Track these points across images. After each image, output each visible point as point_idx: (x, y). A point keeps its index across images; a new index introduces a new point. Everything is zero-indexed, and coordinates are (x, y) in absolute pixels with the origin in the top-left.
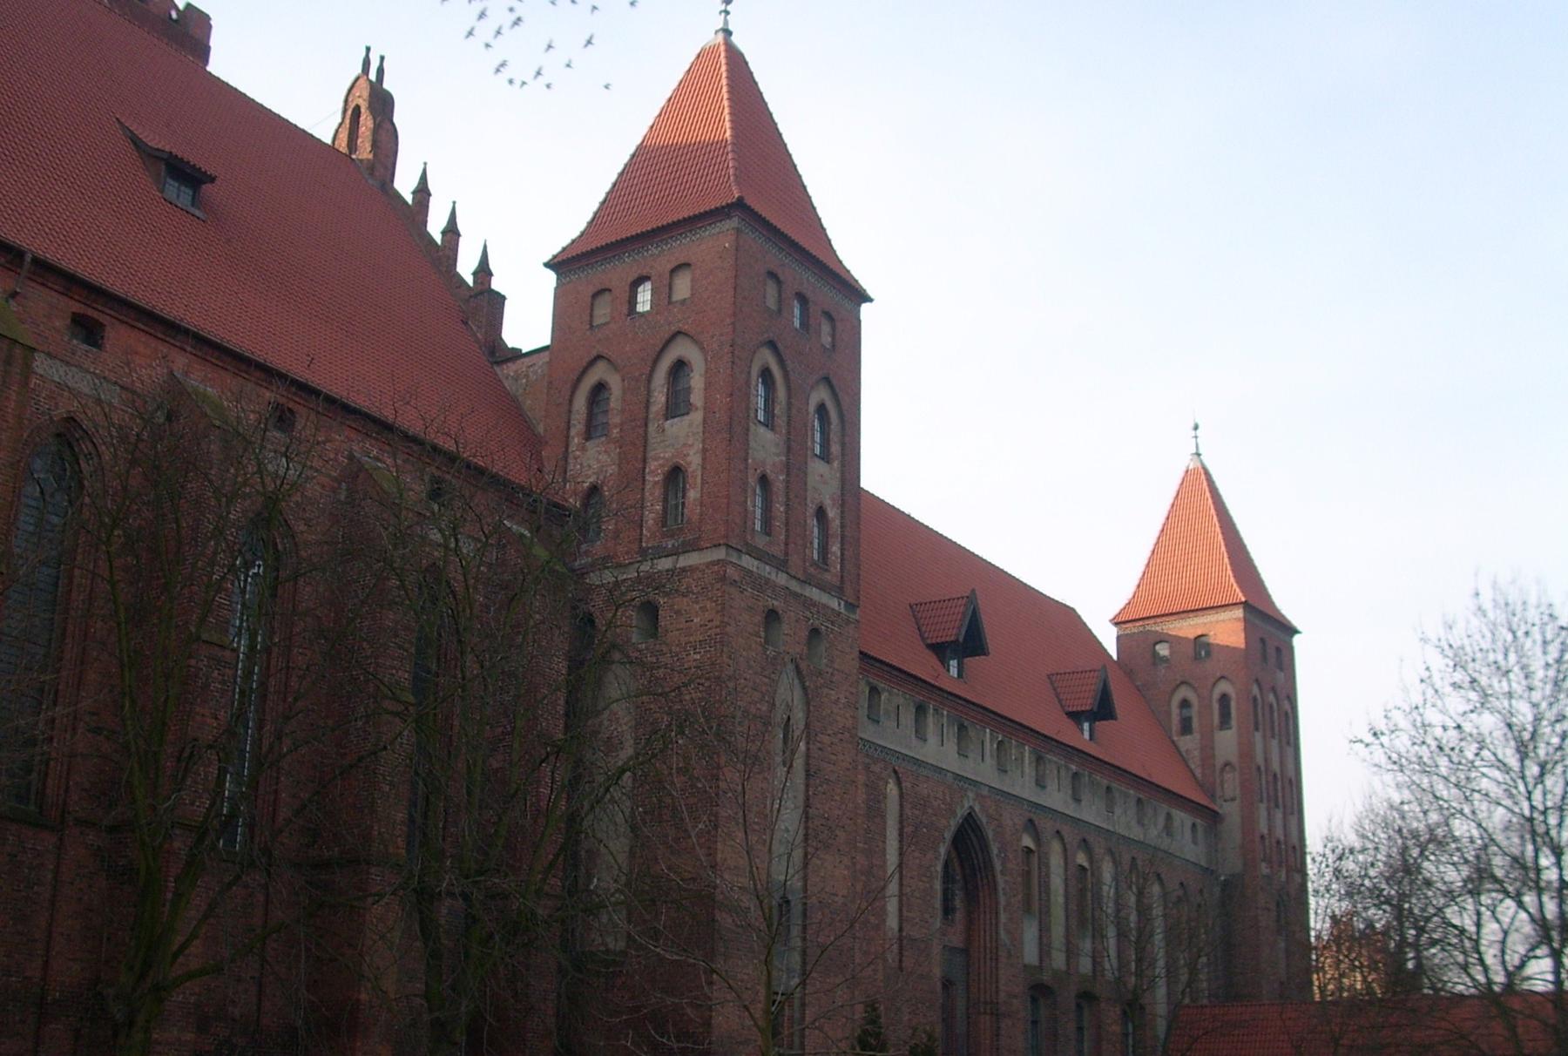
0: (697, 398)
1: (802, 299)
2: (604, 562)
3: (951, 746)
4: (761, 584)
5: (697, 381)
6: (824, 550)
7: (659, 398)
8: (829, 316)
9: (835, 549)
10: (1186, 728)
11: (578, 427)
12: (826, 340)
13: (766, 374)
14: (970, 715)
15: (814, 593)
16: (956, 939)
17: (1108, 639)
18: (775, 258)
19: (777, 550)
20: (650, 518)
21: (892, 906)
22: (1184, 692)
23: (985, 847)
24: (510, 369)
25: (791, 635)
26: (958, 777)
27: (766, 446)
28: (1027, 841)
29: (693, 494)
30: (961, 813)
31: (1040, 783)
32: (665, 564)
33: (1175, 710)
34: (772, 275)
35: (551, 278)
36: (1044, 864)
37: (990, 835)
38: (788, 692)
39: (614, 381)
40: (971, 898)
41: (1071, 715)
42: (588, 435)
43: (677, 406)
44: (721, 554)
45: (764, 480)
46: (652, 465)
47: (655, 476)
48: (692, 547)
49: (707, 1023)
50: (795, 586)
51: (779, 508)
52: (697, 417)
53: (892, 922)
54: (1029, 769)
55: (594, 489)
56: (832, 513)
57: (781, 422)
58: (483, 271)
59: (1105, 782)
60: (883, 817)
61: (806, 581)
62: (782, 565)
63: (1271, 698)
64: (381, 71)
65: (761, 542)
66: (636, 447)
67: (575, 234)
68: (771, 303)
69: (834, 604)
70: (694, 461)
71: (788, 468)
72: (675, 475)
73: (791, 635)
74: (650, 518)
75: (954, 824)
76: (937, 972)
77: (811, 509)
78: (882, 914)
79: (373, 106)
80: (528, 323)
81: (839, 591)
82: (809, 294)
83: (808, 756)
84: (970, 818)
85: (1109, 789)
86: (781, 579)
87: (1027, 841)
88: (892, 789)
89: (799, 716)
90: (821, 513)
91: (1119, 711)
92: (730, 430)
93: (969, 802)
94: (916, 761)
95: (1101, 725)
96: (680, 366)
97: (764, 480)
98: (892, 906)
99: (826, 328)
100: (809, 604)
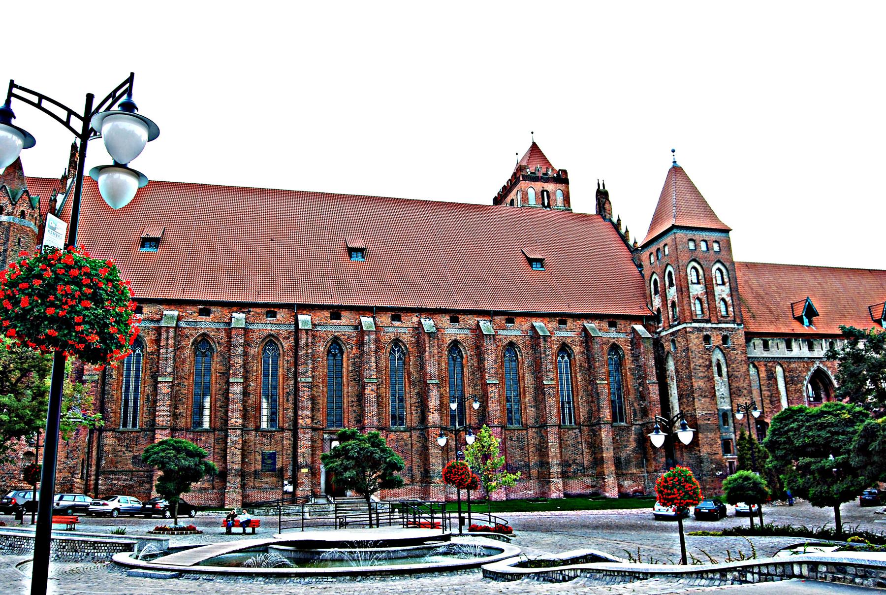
1: (706, 241)
3: (805, 349)
4: (700, 330)
6: (727, 311)
9: (731, 309)
11: (653, 292)
18: (690, 234)
19: (706, 318)
20: (670, 317)
25: (716, 340)
26: (809, 358)
34: (691, 240)
38: (718, 356)
42: (655, 294)
43: (671, 285)
44: (684, 325)
45: (698, 299)
48: (679, 324)
49: (699, 451)
50: (714, 326)
51: (705, 305)
52: (675, 287)
55: (659, 309)
56: (728, 299)
57: (702, 281)
60: (776, 379)
62: (708, 321)
65: (699, 317)
69: (732, 326)
71: (706, 293)
72: (673, 303)
73: (716, 340)
74: (670, 317)
81: (734, 322)
83: (728, 372)
86: (709, 325)
89: (722, 361)
90: (723, 300)
96: (670, 273)
97: (698, 299)
100: (720, 329)
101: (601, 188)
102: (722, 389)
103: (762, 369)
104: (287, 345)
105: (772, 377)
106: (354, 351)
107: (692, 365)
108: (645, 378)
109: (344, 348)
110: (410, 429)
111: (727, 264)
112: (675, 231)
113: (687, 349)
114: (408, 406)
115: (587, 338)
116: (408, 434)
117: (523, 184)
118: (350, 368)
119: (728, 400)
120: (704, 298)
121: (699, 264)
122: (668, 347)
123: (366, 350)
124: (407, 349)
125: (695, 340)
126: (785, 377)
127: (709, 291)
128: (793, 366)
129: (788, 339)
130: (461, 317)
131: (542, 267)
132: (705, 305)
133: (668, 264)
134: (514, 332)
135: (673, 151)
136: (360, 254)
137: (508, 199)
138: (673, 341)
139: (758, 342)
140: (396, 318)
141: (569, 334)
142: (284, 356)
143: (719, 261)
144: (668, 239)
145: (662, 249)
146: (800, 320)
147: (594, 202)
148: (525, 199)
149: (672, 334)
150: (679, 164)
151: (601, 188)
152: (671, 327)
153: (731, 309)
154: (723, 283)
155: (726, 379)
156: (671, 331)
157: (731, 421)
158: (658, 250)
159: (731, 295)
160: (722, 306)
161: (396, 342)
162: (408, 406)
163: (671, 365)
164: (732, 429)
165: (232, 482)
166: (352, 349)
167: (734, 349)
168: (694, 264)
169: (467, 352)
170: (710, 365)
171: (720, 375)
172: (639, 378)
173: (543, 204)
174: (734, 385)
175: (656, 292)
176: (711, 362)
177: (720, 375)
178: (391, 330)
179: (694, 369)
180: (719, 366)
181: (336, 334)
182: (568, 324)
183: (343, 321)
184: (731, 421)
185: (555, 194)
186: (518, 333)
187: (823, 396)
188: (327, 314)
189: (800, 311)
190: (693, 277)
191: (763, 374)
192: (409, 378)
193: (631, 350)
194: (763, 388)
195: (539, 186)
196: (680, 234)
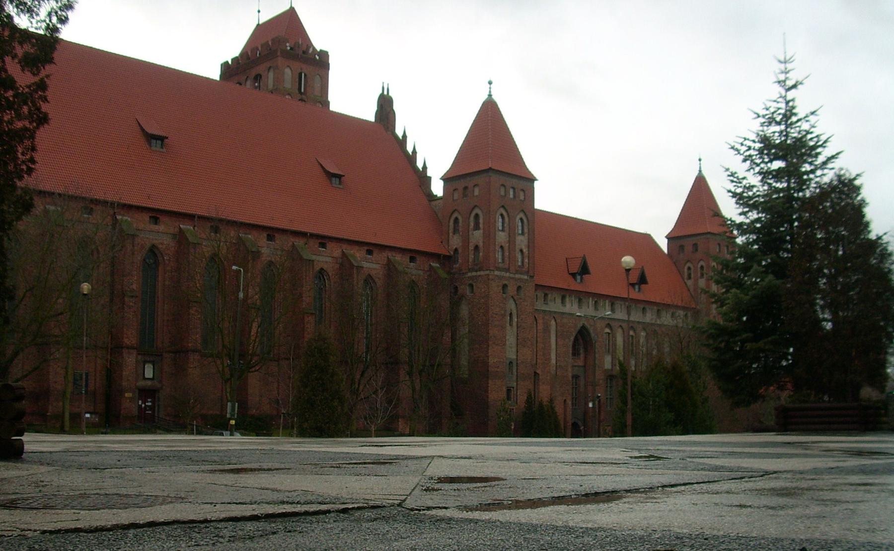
0: (481, 226)
1: (514, 188)
5: (481, 221)
6: (523, 262)
7: (472, 224)
8: (523, 190)
9: (526, 260)
10: (689, 278)
11: (451, 231)
12: (522, 198)
13: (502, 215)
14: (581, 296)
15: (517, 276)
16: (580, 362)
19: (507, 266)
20: (471, 260)
21: (553, 357)
22: (689, 264)
23: (589, 334)
24: (434, 203)
25: (512, 290)
28: (607, 330)
29: (481, 254)
32: (474, 274)
33: (686, 270)
34: (502, 185)
35: (442, 183)
36: (614, 337)
37: (591, 331)
38: (511, 305)
39: (460, 218)
40: (586, 350)
43: (477, 227)
44: (488, 272)
45: (502, 247)
46: (471, 244)
47: (471, 248)
48: (480, 269)
49: (488, 397)
50: (512, 275)
51: (507, 254)
53: (554, 361)
55: (456, 250)
57: (507, 229)
58: (425, 167)
59: (642, 306)
60: (550, 332)
61: (517, 272)
62: (507, 270)
65: (501, 265)
66: (466, 240)
67: (448, 168)
68: (503, 193)
70: (481, 244)
71: (509, 242)
72: (477, 248)
73: (512, 290)
74: (471, 260)
76: (570, 375)
77: (518, 250)
78: (549, 359)
79: (385, 104)
80: (437, 188)
84: (583, 327)
85: (644, 309)
86: (508, 274)
87: (607, 330)
88: (553, 322)
89: (514, 312)
90: (521, 251)
94: (563, 313)
95: (643, 286)
96: (477, 216)
97: (502, 247)
98: (553, 357)
99: (522, 194)
101: (385, 93)
102: (511, 339)
103: (540, 321)
105: (547, 330)
109: (160, 259)
119: (514, 350)
120: (506, 246)
121: (506, 211)
125: (495, 287)
128: (565, 321)
129: (564, 293)
131: (340, 184)
132: (507, 254)
133: (476, 206)
134: (325, 259)
135: (490, 83)
136: (159, 142)
138: (471, 286)
139: (541, 294)
141: (375, 266)
144: (481, 180)
146: (574, 275)
147: (374, 108)
148: (279, 80)
150: (495, 97)
151: (385, 93)
153: (526, 260)
154: (523, 233)
155: (515, 329)
157: (515, 371)
158: (466, 188)
159: (529, 247)
163: (464, 310)
164: (515, 378)
166: (169, 260)
170: (504, 316)
171: (511, 325)
175: (455, 231)
176: (505, 311)
177: (511, 325)
180: (511, 314)
181: (155, 242)
182: (375, 254)
183: (161, 228)
184: (515, 371)
187: (581, 351)
188: (146, 217)
189: (575, 268)
191: (540, 327)
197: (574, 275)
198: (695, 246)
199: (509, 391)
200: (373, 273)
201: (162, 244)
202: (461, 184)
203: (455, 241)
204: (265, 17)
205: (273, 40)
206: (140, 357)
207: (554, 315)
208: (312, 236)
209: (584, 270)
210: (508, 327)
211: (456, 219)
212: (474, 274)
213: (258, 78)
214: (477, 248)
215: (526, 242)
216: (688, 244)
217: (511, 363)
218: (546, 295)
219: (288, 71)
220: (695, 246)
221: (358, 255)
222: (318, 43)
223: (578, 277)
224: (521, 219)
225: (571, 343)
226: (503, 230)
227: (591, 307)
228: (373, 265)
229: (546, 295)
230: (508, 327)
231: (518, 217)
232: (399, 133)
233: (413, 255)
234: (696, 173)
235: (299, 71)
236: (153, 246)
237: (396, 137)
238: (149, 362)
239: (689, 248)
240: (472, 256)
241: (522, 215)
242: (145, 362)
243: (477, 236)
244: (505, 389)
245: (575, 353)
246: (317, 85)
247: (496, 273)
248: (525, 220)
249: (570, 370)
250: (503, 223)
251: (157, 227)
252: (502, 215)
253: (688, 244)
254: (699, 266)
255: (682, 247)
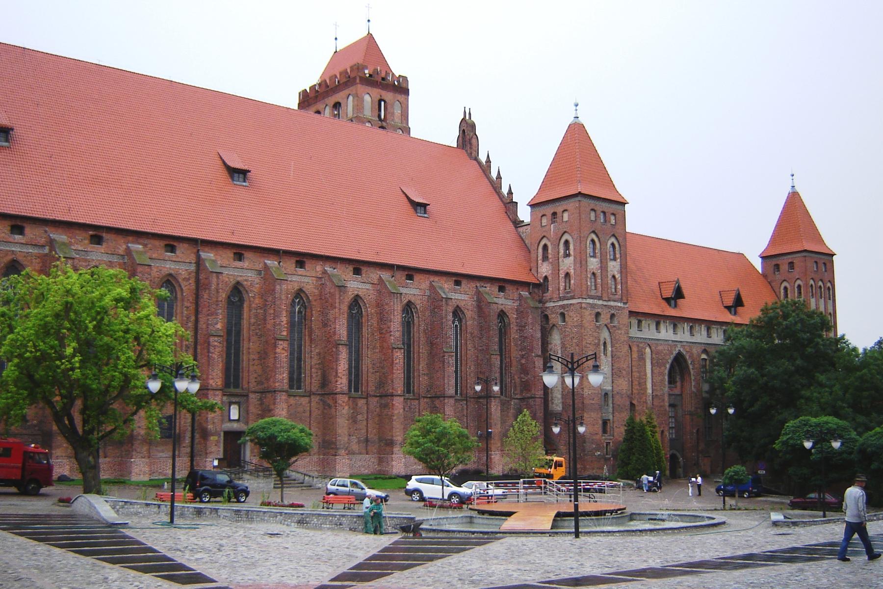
0: (572, 252)
1: (604, 213)
2: (551, 300)
3: (671, 331)
4: (593, 306)
8: (613, 214)
9: (619, 287)
11: (540, 257)
12: (613, 222)
13: (593, 241)
14: (676, 322)
15: (612, 303)
17: (758, 264)
19: (599, 294)
20: (562, 288)
21: (649, 385)
22: (785, 284)
23: (685, 361)
24: (521, 230)
25: (605, 319)
27: (593, 264)
30: (675, 353)
31: (709, 336)
32: (566, 302)
34: (592, 210)
35: (529, 208)
38: (605, 334)
39: (549, 244)
41: (726, 307)
43: (567, 255)
44: (580, 300)
46: (561, 272)
47: (562, 275)
48: (573, 298)
50: (605, 303)
52: (572, 258)
53: (650, 391)
54: (704, 333)
55: (546, 277)
56: (618, 276)
57: (598, 255)
58: (510, 193)
63: (820, 283)
64: (470, 114)
65: (593, 293)
66: (556, 268)
68: (593, 218)
69: (619, 304)
70: (572, 272)
72: (567, 275)
73: (605, 319)
74: (562, 288)
75: (672, 357)
76: (667, 404)
77: (610, 277)
78: (646, 389)
80: (524, 214)
81: (621, 300)
82: (606, 210)
83: (612, 351)
86: (600, 302)
88: (648, 350)
90: (614, 277)
91: (745, 303)
92: (582, 262)
93: (679, 348)
95: (740, 309)
96: (567, 243)
97: (594, 274)
98: (649, 385)
99: (612, 218)
101: (467, 117)
103: (635, 349)
104: (187, 288)
105: (642, 358)
106: (257, 301)
107: (584, 343)
108: (531, 350)
109: (245, 296)
110: (310, 394)
111: (621, 239)
112: (579, 198)
113: (581, 326)
114: (308, 367)
115: (481, 305)
116: (307, 399)
117: (360, 88)
118: (253, 320)
122: (555, 319)
123: (278, 303)
124: (309, 301)
125: (588, 315)
126: (652, 359)
127: (603, 267)
128: (660, 348)
129: (658, 319)
130: (364, 269)
134: (414, 291)
135: (577, 105)
136: (241, 176)
137: (332, 100)
139: (634, 322)
140: (301, 264)
142: (183, 300)
143: (614, 235)
144: (571, 205)
145: (559, 215)
146: (668, 300)
147: (456, 133)
148: (359, 107)
149: (563, 307)
150: (582, 120)
151: (467, 117)
152: (561, 299)
153: (619, 287)
154: (615, 259)
156: (561, 303)
157: (610, 402)
158: (554, 214)
159: (621, 272)
160: (610, 281)
161: (299, 293)
162: (308, 367)
163: (556, 339)
164: (611, 410)
165: (138, 450)
167: (619, 329)
168: (594, 236)
169: (369, 310)
170: (598, 345)
171: (605, 354)
172: (521, 350)
173: (379, 116)
174: (616, 365)
175: (545, 258)
176: (599, 340)
177: (605, 354)
178: (294, 278)
179: (586, 347)
180: (605, 343)
181: (239, 279)
182: (463, 285)
183: (245, 264)
184: (610, 402)
185: (393, 106)
186: (416, 292)
187: (678, 379)
190: (590, 250)
191: (635, 355)
192: (310, 335)
193: (517, 319)
194: (634, 369)
195: (376, 93)
196: (585, 202)
197: (668, 300)
198: (791, 265)
199: (605, 423)
200: (461, 304)
201: (246, 280)
202: (549, 210)
203: (545, 269)
204: (342, 45)
205: (351, 68)
206: (225, 398)
207: (649, 343)
208: (400, 268)
209: (679, 294)
210: (602, 356)
211: (545, 247)
212: (566, 302)
213: (337, 105)
214: (567, 275)
215: (618, 267)
216: (784, 263)
217: (606, 394)
218: (640, 322)
219: (367, 98)
220: (791, 265)
221: (446, 287)
222: (397, 68)
223: (673, 302)
224: (613, 244)
225: (667, 372)
226: (594, 256)
227: (687, 333)
228: (463, 296)
229: (640, 322)
230: (602, 356)
231: (610, 242)
232: (483, 158)
233: (502, 284)
234: (789, 190)
235: (379, 97)
236: (238, 283)
237: (479, 163)
238: (235, 403)
239: (784, 267)
240: (562, 285)
241: (613, 240)
242: (230, 403)
243: (567, 264)
244: (601, 422)
245: (672, 381)
246: (398, 111)
247: (591, 301)
248: (617, 245)
249: (666, 398)
250: (594, 249)
251: (239, 264)
252: (593, 241)
253: (784, 263)
254: (796, 285)
255: (777, 267)
